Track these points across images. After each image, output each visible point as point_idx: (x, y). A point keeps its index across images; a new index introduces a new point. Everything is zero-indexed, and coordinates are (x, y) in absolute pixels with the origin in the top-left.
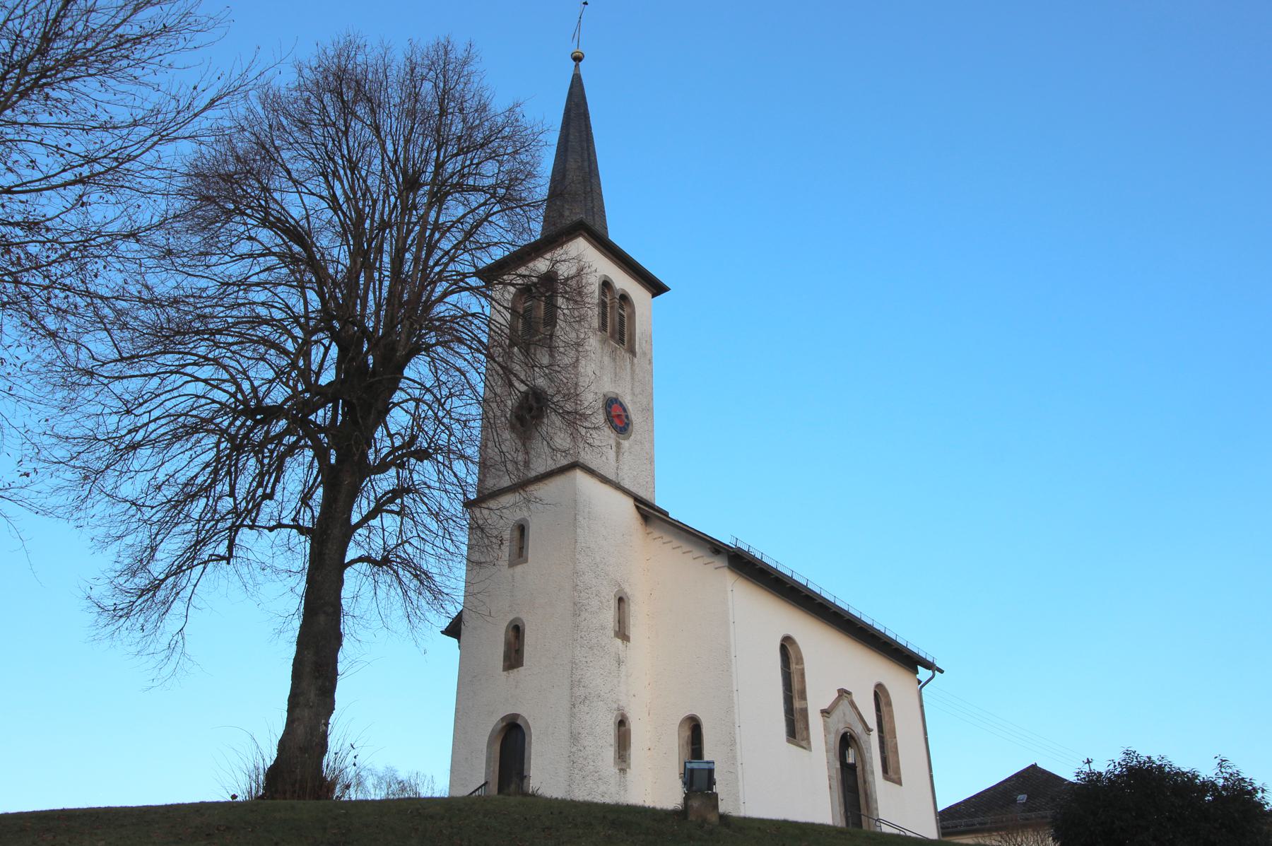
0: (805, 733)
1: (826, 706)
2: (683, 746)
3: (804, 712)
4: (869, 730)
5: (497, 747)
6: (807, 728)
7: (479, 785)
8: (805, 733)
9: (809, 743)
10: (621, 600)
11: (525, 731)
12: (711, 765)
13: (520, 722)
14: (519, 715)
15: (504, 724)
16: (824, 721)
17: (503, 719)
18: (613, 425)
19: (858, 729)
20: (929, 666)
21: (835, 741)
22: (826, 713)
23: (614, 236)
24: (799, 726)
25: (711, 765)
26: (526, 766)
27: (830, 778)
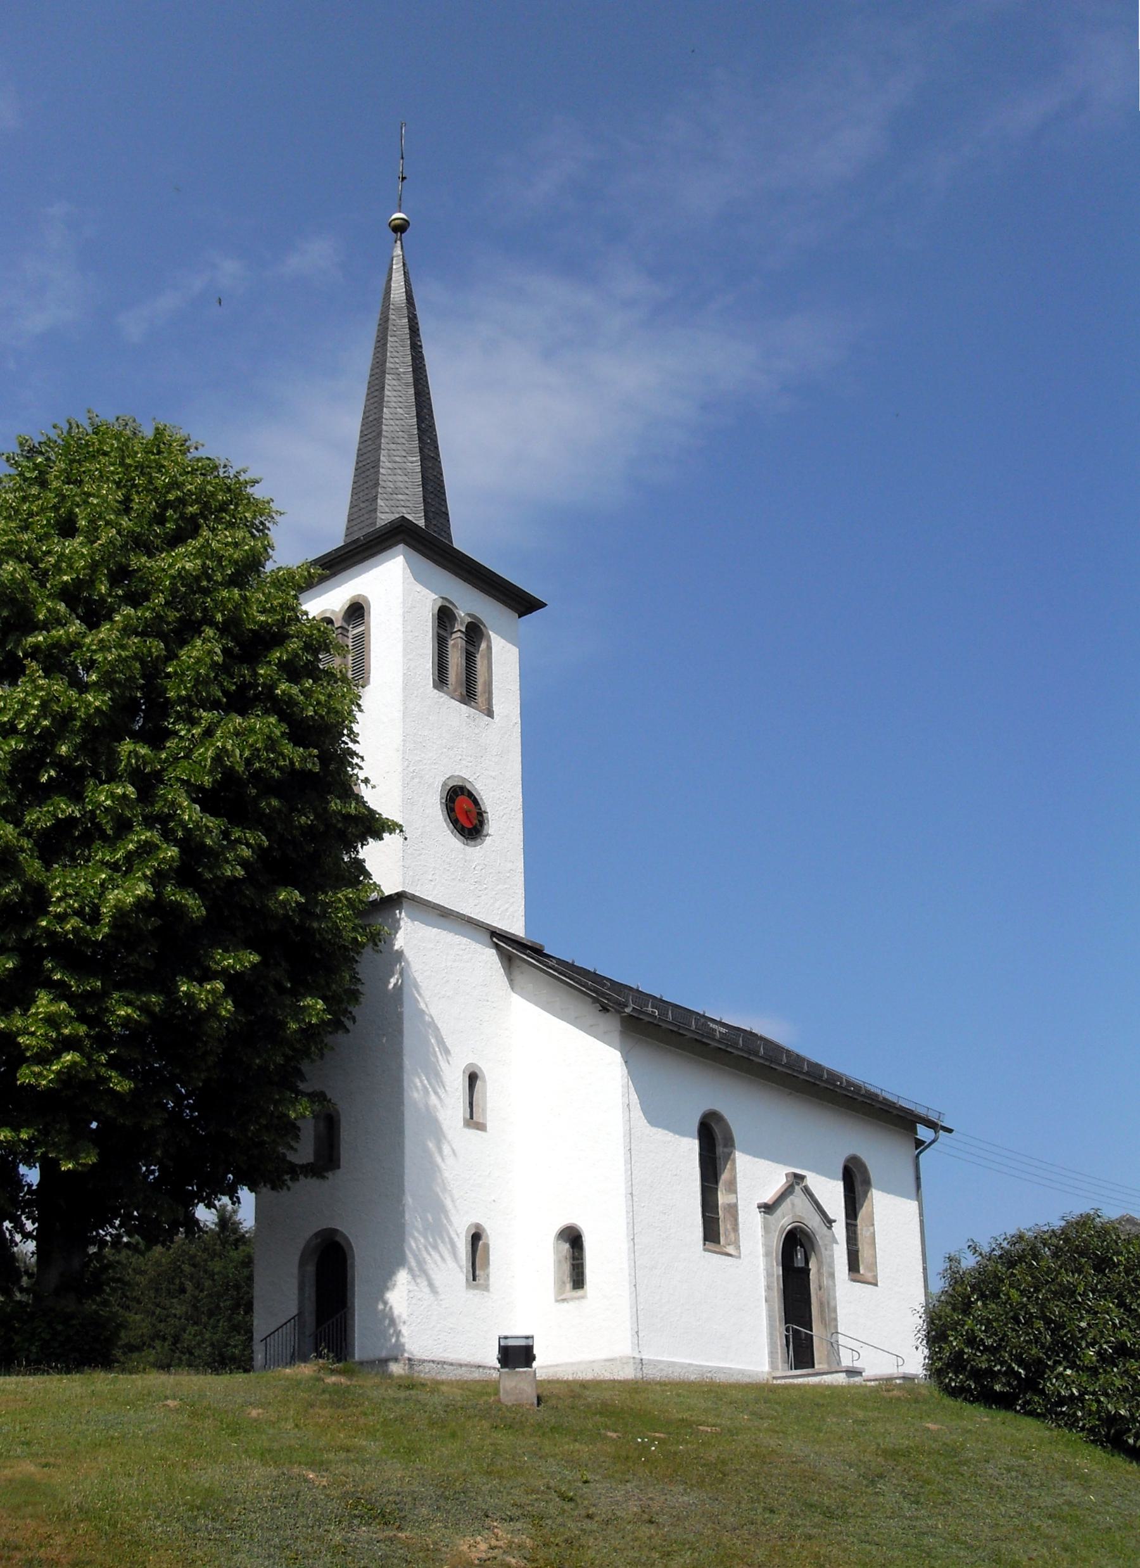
0: (732, 1236)
1: (768, 1197)
2: (559, 1262)
3: (733, 1209)
4: (829, 1222)
5: (311, 1269)
6: (735, 1228)
7: (280, 1325)
8: (732, 1236)
9: (738, 1248)
10: (473, 1078)
11: (346, 1249)
12: (529, 1342)
13: (338, 1239)
14: (337, 1230)
15: (319, 1240)
16: (765, 1218)
17: (317, 1235)
18: (459, 826)
19: (813, 1222)
20: (932, 1125)
21: (777, 1244)
22: (767, 1209)
23: (462, 540)
24: (724, 1227)
25: (530, 1340)
26: (349, 1294)
27: (769, 1288)
